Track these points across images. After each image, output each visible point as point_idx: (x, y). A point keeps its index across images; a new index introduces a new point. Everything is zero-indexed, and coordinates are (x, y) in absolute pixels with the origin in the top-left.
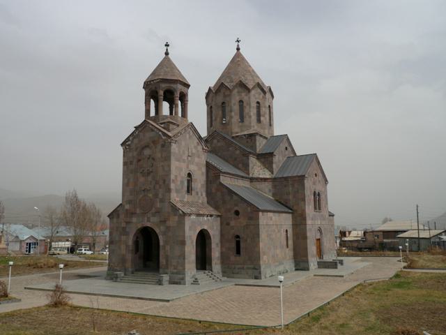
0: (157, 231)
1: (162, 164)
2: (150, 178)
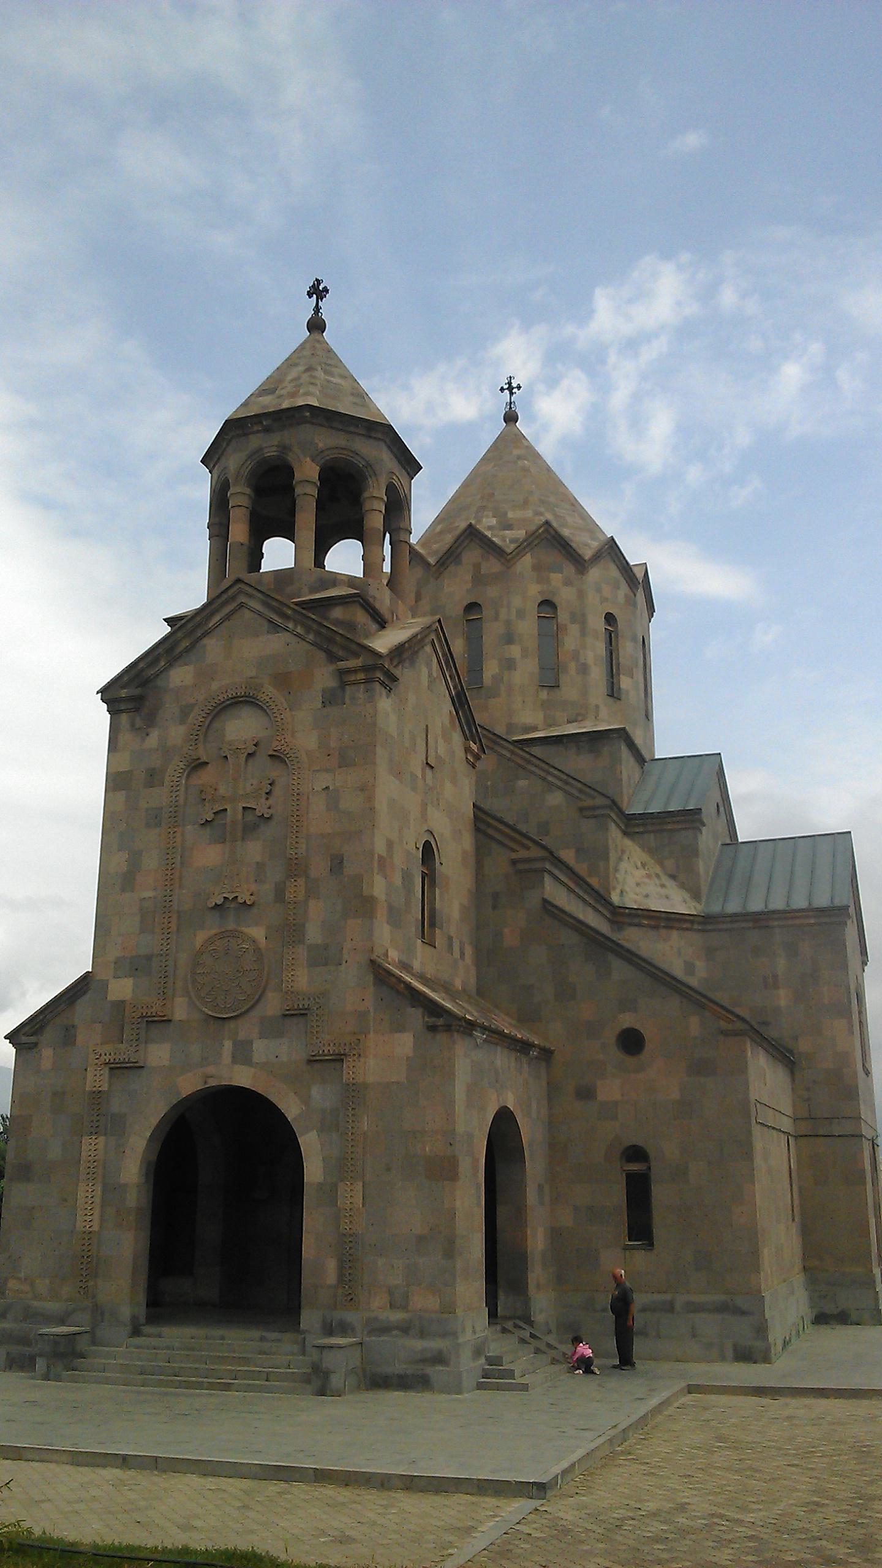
0: (291, 1108)
1: (323, 780)
2: (254, 850)
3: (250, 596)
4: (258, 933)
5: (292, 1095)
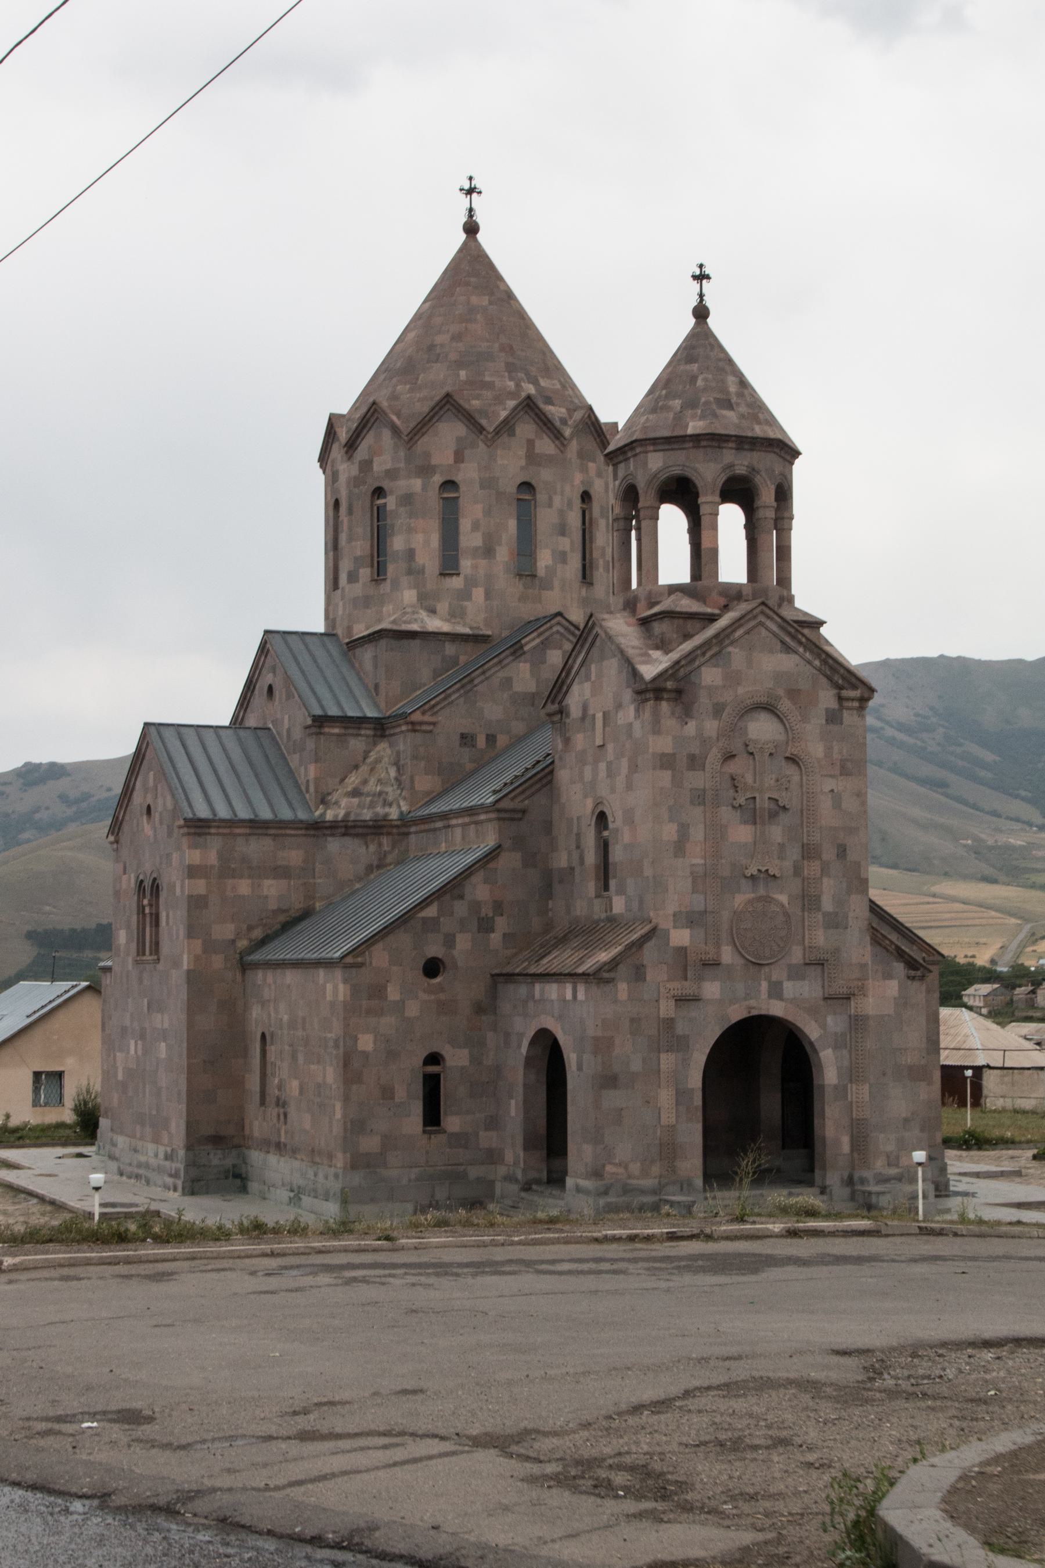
0: (812, 1031)
1: (829, 784)
2: (776, 833)
3: (768, 617)
4: (783, 898)
5: (813, 1023)
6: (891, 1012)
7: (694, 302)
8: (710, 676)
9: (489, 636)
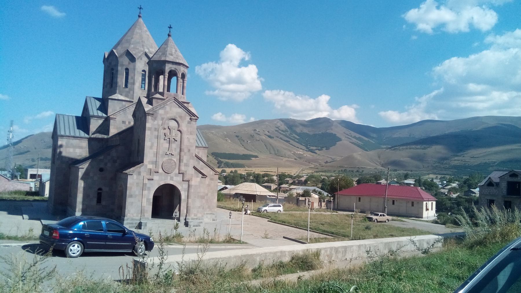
0: (179, 187)
1: (188, 136)
4: (175, 160)
6: (198, 185)
7: (168, 32)
8: (161, 112)
9: (133, 101)
